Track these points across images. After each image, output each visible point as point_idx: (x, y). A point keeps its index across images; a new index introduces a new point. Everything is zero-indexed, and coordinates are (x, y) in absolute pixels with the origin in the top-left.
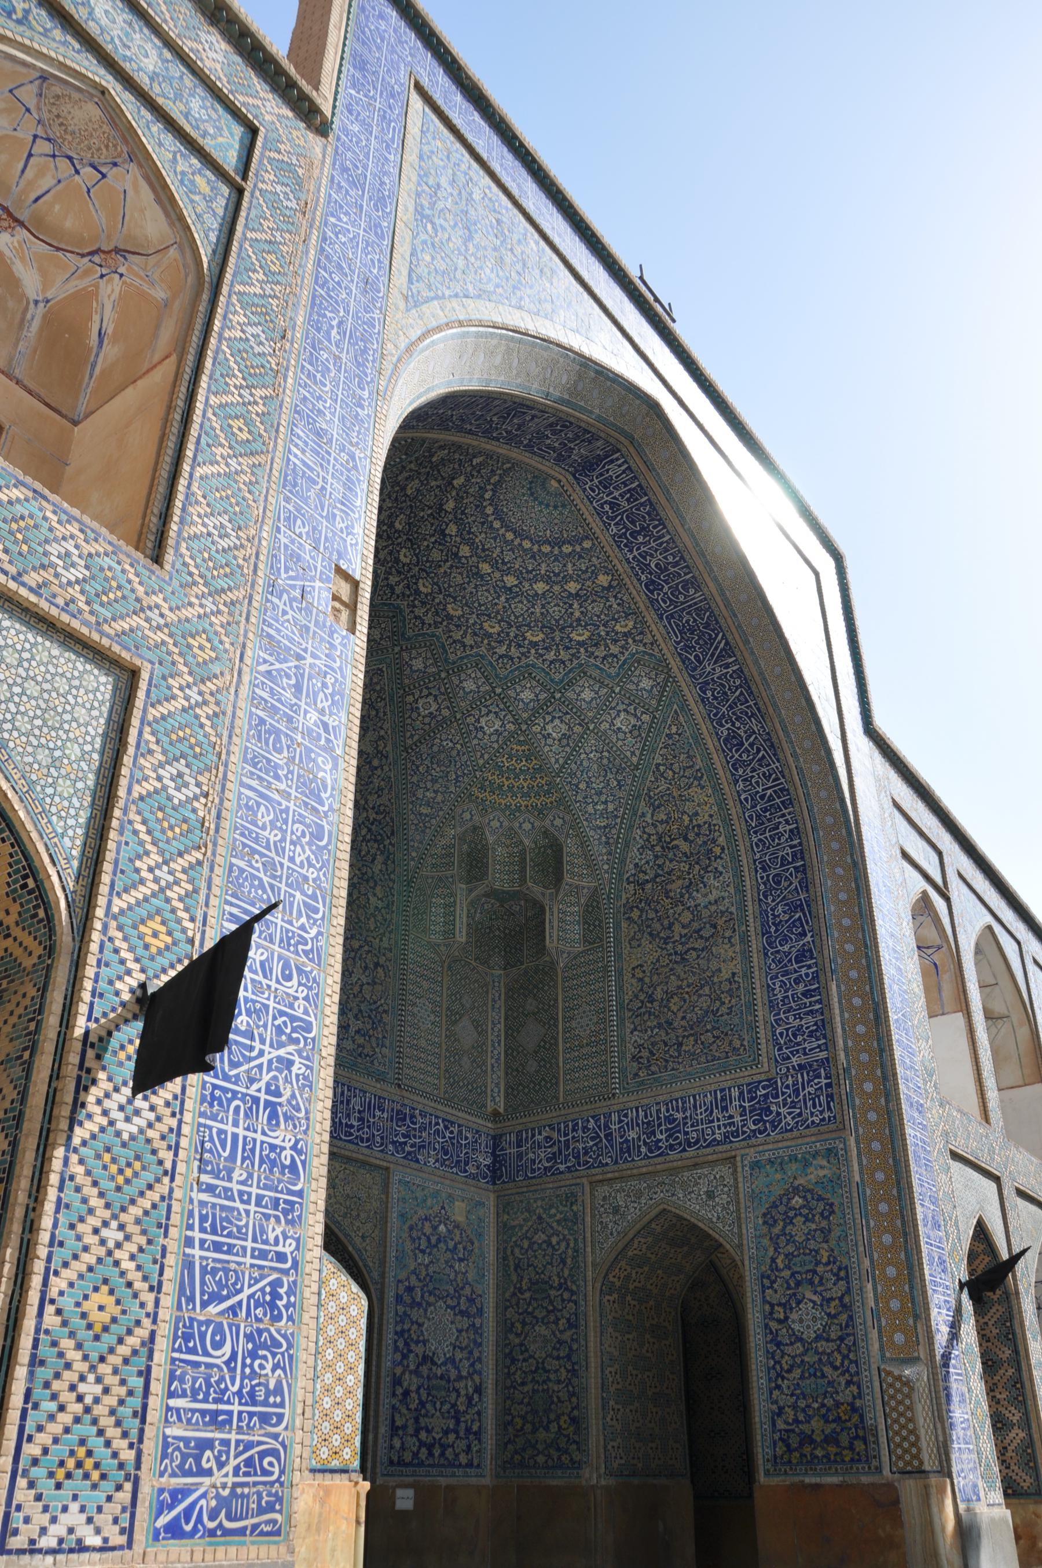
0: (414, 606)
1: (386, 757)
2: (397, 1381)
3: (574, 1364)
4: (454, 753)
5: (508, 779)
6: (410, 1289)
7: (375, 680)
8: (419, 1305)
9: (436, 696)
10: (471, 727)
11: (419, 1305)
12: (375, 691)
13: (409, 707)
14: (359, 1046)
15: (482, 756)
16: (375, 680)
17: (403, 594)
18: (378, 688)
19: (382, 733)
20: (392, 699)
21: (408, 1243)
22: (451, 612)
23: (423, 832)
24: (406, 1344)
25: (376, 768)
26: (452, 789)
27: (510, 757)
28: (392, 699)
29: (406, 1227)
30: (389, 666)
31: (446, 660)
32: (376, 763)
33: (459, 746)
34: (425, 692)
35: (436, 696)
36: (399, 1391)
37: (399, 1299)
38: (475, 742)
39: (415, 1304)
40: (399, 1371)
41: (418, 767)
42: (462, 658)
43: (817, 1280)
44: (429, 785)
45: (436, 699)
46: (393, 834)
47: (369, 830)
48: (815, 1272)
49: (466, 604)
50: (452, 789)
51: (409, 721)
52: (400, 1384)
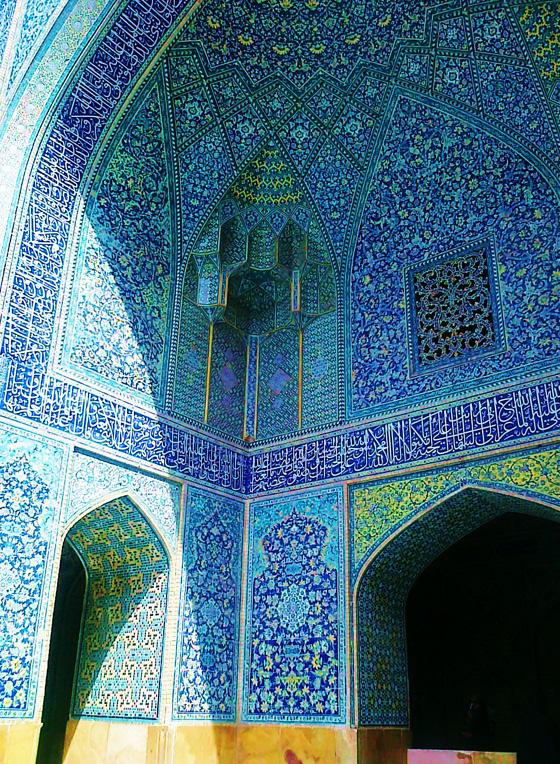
0: (366, 53)
1: (471, 131)
3: (231, 635)
4: (502, 74)
5: (552, 38)
7: (406, 109)
9: (448, 66)
10: (487, 49)
12: (414, 112)
13: (445, 91)
14: (544, 348)
15: (517, 53)
16: (406, 109)
17: (351, 58)
18: (414, 109)
19: (450, 123)
20: (430, 102)
22: (386, 23)
23: (548, 138)
25: (471, 144)
26: (530, 93)
27: (531, 27)
28: (430, 102)
30: (402, 92)
31: (422, 44)
32: (467, 142)
33: (498, 68)
34: (440, 72)
35: (448, 66)
38: (502, 52)
41: (497, 110)
42: (427, 30)
43: (20, 547)
44: (517, 109)
45: (451, 67)
46: (527, 164)
47: (503, 183)
48: (20, 540)
49: (385, 9)
50: (530, 93)
51: (457, 97)
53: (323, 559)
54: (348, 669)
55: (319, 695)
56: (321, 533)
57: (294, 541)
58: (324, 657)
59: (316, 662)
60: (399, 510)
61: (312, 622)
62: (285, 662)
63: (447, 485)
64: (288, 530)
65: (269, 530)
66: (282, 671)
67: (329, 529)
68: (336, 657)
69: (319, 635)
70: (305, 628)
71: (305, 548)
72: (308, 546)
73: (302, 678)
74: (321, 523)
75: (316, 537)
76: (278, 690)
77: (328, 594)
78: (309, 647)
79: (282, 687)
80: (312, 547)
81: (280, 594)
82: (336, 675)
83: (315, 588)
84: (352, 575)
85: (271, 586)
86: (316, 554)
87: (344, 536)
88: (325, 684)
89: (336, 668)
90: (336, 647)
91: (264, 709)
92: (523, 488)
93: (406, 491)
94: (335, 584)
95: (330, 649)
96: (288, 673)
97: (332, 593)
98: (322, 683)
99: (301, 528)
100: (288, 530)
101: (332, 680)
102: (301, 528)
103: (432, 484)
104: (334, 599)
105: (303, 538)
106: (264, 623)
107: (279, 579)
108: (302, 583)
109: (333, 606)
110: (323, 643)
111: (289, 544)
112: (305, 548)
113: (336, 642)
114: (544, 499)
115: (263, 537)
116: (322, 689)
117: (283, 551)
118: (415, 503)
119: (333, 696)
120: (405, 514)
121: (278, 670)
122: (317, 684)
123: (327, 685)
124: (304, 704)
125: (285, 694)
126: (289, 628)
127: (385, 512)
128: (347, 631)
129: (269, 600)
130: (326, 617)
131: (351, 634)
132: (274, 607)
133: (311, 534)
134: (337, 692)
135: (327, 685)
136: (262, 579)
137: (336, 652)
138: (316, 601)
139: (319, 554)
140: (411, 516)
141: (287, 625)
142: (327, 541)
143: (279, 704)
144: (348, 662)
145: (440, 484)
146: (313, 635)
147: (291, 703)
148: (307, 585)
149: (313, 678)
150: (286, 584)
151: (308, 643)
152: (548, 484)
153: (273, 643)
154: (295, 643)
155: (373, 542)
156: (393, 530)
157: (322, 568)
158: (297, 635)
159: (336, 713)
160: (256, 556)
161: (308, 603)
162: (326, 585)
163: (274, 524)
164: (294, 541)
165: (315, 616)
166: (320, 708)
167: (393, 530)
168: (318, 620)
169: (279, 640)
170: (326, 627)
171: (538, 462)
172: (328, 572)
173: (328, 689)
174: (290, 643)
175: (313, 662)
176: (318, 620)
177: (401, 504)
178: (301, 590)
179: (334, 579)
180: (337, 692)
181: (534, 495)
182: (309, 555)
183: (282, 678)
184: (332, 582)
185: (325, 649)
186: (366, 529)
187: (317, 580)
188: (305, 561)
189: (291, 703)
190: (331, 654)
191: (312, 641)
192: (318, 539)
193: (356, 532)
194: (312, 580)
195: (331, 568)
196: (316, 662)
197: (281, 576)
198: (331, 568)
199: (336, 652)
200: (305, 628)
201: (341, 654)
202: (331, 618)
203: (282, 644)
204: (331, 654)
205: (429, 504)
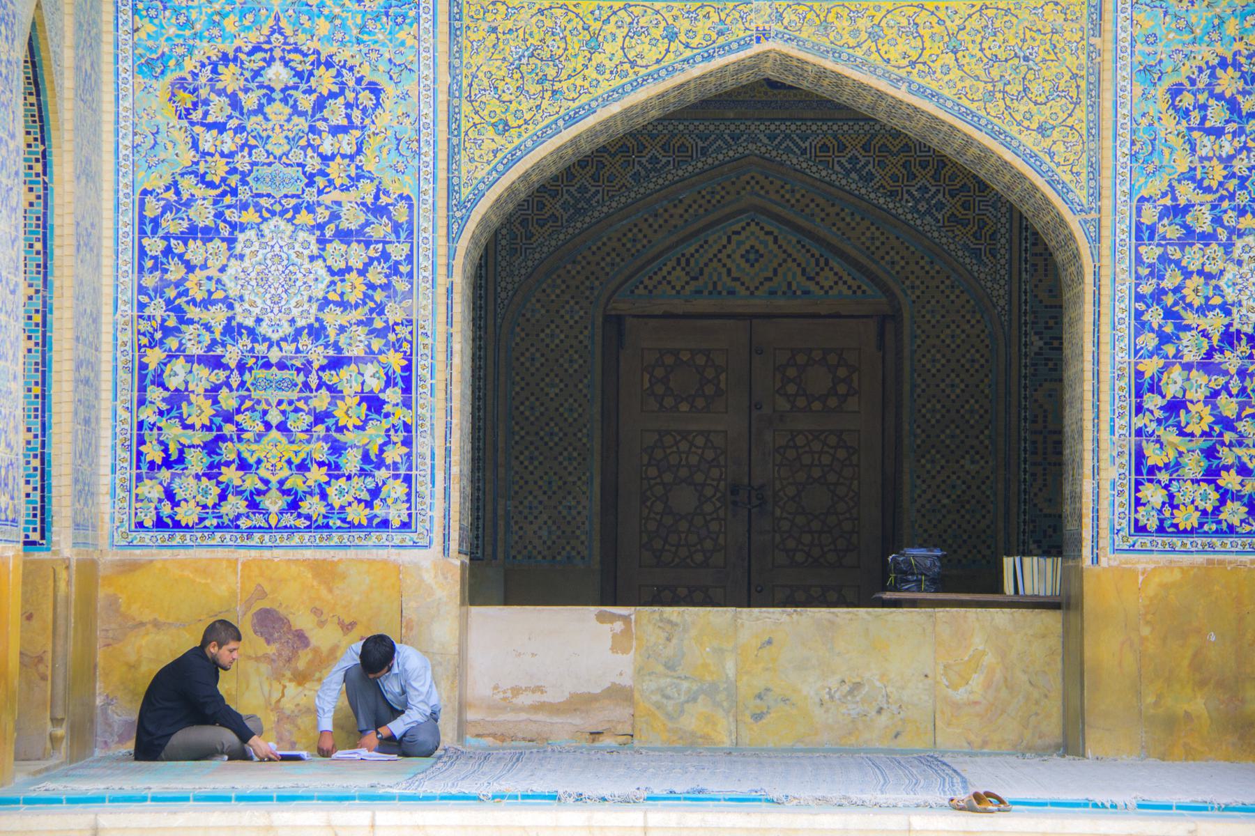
2: (1144, 386)
6: (1177, 211)
8: (1207, 238)
11: (1207, 238)
21: (1169, 121)
24: (1169, 314)
29: (1161, 91)
36: (1153, 402)
37: (1144, 233)
39: (1190, 236)
40: (1150, 367)
52: (1155, 388)
53: (369, 162)
54: (440, 430)
55: (359, 487)
56: (366, 98)
57: (277, 106)
58: (374, 403)
59: (349, 411)
60: (591, 73)
61: (333, 318)
62: (252, 409)
63: (720, 33)
64: (257, 73)
65: (189, 65)
66: (241, 431)
67: (390, 90)
68: (407, 404)
69: (358, 351)
70: (317, 332)
71: (312, 129)
72: (321, 125)
73: (307, 448)
74: (365, 71)
75: (348, 105)
76: (230, 475)
77: (385, 256)
78: (326, 376)
79: (243, 466)
80: (336, 130)
81: (231, 241)
82: (407, 442)
83: (345, 236)
84: (457, 207)
85: (203, 214)
86: (349, 150)
87: (433, 112)
88: (371, 462)
89: (407, 428)
90: (407, 381)
91: (187, 514)
92: (903, 73)
93: (610, 28)
94: (404, 231)
95: (389, 382)
96: (259, 438)
97: (398, 251)
98: (366, 458)
99: (299, 75)
100: (257, 73)
101: (394, 454)
102: (299, 75)
103: (684, 24)
104: (404, 269)
105: (306, 103)
106: (179, 310)
107: (228, 200)
108: (304, 218)
109: (400, 285)
110: (370, 369)
111: (260, 110)
112: (312, 129)
113: (407, 368)
114: (942, 106)
115: (170, 77)
116: (363, 473)
117: (240, 129)
118: (633, 64)
119: (396, 489)
120: (604, 87)
121: (229, 429)
122: (351, 461)
123: (380, 463)
124: (312, 506)
125: (251, 482)
126: (264, 329)
127: (551, 72)
128: (441, 347)
129: (195, 251)
130: (380, 310)
131: (450, 353)
132: (213, 272)
133: (333, 95)
134: (408, 479)
135: (380, 463)
136: (170, 195)
137: (407, 390)
138: (349, 269)
139: (359, 151)
140: (621, 92)
141: (259, 321)
142: (383, 119)
143: (235, 505)
144: (440, 415)
145: (703, 27)
146: (340, 350)
147: (274, 502)
148: (321, 227)
149: (337, 449)
150: (250, 216)
151: (322, 368)
152: (955, 74)
153: (216, 363)
154: (282, 366)
155: (514, 140)
156: (572, 119)
157: (366, 190)
158: (289, 348)
159: (405, 525)
160: (144, 127)
161: (323, 272)
162: (380, 229)
163: (207, 49)
164: (277, 106)
165: (343, 305)
166: (357, 514)
167: (572, 119)
168: (359, 314)
169: (232, 355)
170: (381, 333)
171: (941, 22)
172: (384, 200)
173: (382, 474)
174: (267, 365)
175: (339, 413)
176: (359, 314)
177: (597, 58)
178: (302, 235)
179: (403, 219)
180: (408, 479)
181: (922, 91)
182: (326, 149)
183: (242, 447)
184: (397, 228)
185: (375, 384)
186: (494, 105)
187: (352, 218)
188: (313, 164)
189: (274, 502)
190: (393, 396)
191: (336, 363)
192: (356, 114)
193: (466, 108)
194: (335, 217)
195: (395, 190)
196: (349, 411)
197: (234, 192)
198: (395, 190)
199: (407, 390)
200: (317, 332)
201: (420, 392)
202: (394, 313)
203: (242, 367)
204: (393, 396)
205: (671, 71)
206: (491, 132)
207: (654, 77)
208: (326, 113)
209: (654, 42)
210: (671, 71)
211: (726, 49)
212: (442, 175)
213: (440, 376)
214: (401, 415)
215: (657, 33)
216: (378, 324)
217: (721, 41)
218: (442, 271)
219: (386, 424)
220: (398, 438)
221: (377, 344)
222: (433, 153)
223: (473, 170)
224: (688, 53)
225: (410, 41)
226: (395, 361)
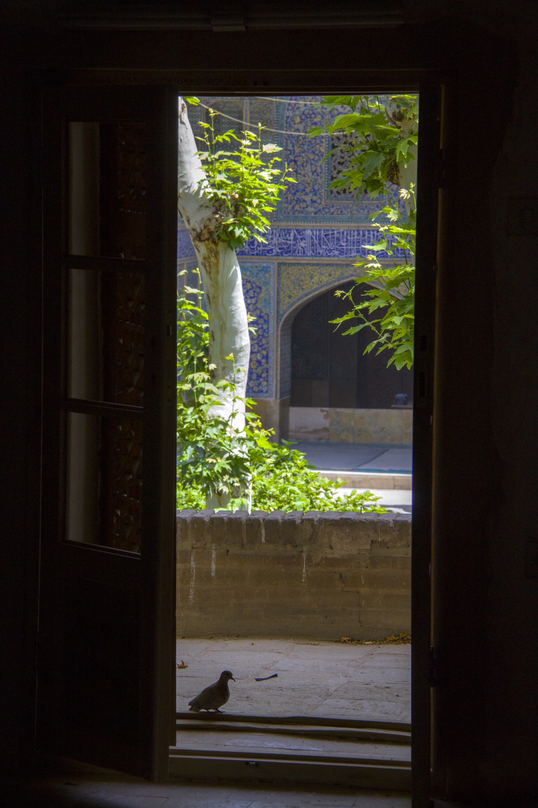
54: (275, 369)
56: (258, 290)
60: (311, 284)
67: (264, 288)
68: (267, 363)
72: (248, 296)
74: (258, 284)
75: (254, 292)
77: (262, 328)
80: (251, 298)
82: (267, 372)
84: (279, 316)
87: (273, 293)
93: (316, 273)
94: (267, 322)
95: (263, 357)
97: (265, 327)
98: (258, 376)
101: (264, 375)
103: (333, 273)
104: (266, 331)
110: (258, 355)
113: (267, 355)
116: (257, 379)
118: (321, 282)
119: (265, 383)
123: (261, 377)
127: (302, 284)
130: (261, 340)
133: (250, 289)
134: (267, 381)
135: (261, 377)
139: (256, 302)
140: (318, 288)
142: (262, 295)
144: (275, 366)
145: (338, 273)
156: (306, 295)
159: (267, 392)
167: (306, 295)
173: (261, 379)
177: (313, 280)
179: (266, 319)
180: (267, 381)
184: (265, 321)
201: (270, 360)
202: (264, 341)
204: (264, 361)
205: (330, 283)
206: (287, 298)
207: (326, 285)
208: (249, 293)
209: (326, 277)
210: (330, 283)
211: (343, 278)
212: (276, 308)
213: (275, 356)
214: (266, 366)
215: (327, 275)
216: (261, 344)
217: (342, 276)
218: (275, 332)
219: (262, 368)
220: (265, 371)
221: (260, 349)
222: (273, 303)
223: (283, 307)
224: (334, 279)
225: (268, 277)
226: (264, 353)
